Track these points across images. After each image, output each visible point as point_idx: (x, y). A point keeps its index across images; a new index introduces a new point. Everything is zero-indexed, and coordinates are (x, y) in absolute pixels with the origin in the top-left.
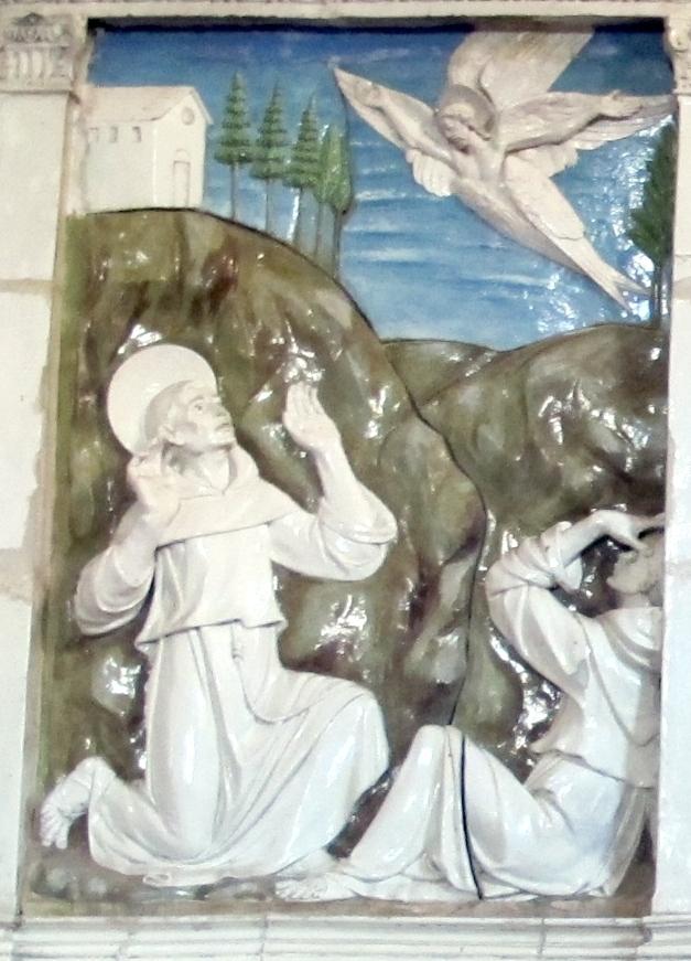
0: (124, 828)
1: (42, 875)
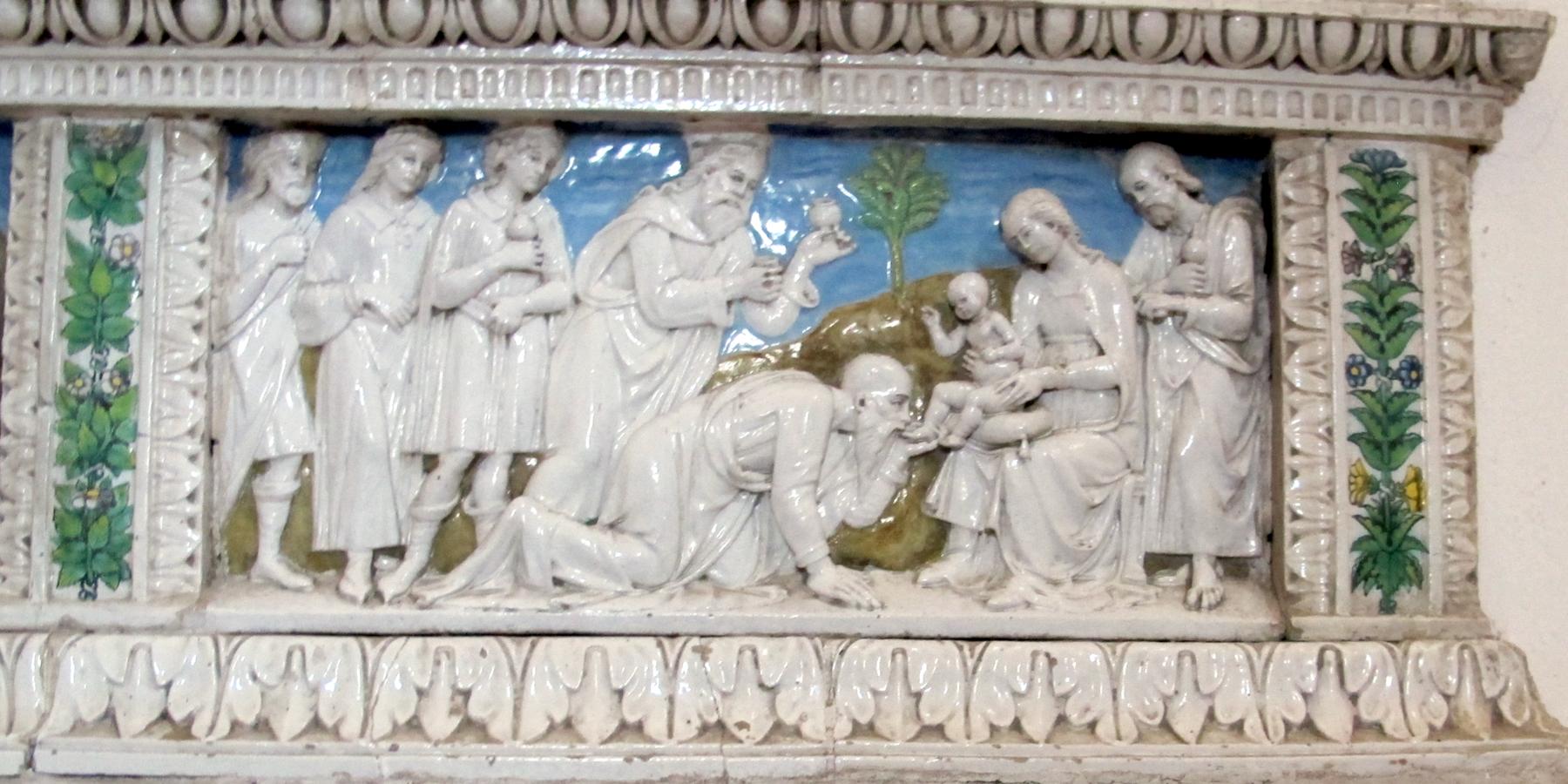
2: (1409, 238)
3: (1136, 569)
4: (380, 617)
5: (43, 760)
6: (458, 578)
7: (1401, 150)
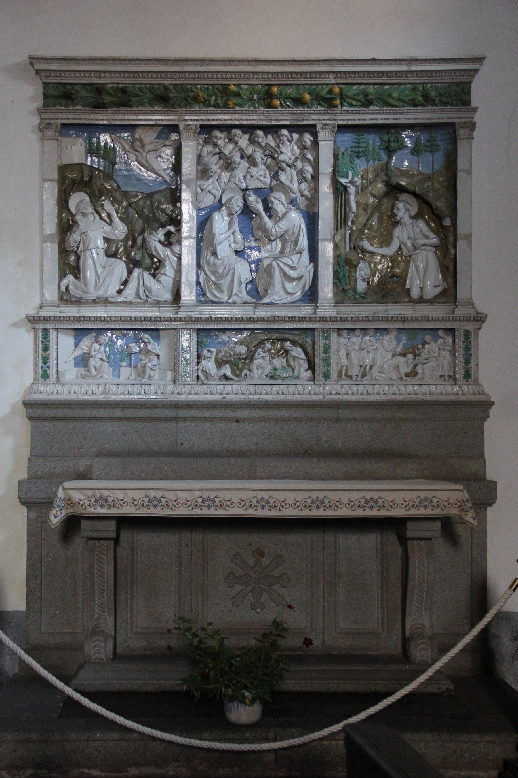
0: (76, 288)
1: (62, 297)
2: (471, 340)
3: (439, 377)
4: (357, 383)
5: (325, 397)
6: (365, 378)
7: (470, 329)
